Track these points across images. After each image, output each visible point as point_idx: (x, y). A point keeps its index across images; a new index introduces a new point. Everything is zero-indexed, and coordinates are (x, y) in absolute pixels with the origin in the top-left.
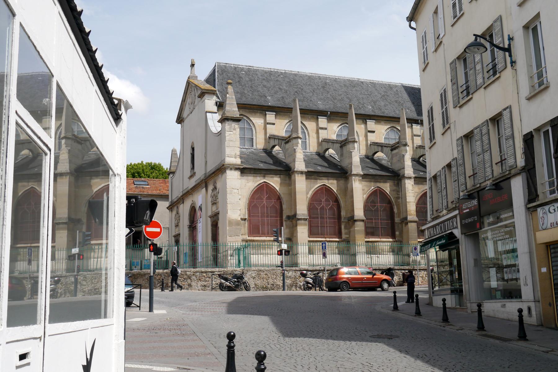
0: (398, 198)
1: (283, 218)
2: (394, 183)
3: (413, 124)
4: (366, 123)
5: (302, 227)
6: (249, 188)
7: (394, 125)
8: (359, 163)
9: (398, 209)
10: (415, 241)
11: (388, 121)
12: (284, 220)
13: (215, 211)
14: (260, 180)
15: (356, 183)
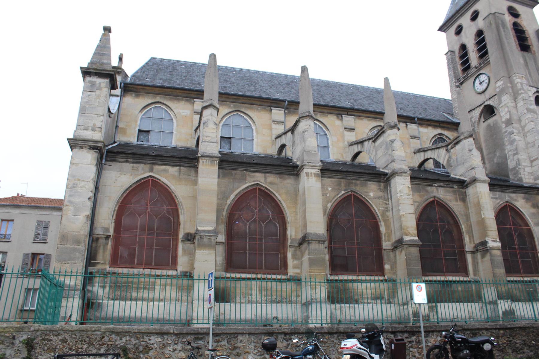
0: (387, 210)
2: (380, 186)
3: (408, 124)
4: (342, 120)
5: (205, 251)
9: (387, 227)
11: (373, 118)
14: (142, 174)
15: (310, 180)
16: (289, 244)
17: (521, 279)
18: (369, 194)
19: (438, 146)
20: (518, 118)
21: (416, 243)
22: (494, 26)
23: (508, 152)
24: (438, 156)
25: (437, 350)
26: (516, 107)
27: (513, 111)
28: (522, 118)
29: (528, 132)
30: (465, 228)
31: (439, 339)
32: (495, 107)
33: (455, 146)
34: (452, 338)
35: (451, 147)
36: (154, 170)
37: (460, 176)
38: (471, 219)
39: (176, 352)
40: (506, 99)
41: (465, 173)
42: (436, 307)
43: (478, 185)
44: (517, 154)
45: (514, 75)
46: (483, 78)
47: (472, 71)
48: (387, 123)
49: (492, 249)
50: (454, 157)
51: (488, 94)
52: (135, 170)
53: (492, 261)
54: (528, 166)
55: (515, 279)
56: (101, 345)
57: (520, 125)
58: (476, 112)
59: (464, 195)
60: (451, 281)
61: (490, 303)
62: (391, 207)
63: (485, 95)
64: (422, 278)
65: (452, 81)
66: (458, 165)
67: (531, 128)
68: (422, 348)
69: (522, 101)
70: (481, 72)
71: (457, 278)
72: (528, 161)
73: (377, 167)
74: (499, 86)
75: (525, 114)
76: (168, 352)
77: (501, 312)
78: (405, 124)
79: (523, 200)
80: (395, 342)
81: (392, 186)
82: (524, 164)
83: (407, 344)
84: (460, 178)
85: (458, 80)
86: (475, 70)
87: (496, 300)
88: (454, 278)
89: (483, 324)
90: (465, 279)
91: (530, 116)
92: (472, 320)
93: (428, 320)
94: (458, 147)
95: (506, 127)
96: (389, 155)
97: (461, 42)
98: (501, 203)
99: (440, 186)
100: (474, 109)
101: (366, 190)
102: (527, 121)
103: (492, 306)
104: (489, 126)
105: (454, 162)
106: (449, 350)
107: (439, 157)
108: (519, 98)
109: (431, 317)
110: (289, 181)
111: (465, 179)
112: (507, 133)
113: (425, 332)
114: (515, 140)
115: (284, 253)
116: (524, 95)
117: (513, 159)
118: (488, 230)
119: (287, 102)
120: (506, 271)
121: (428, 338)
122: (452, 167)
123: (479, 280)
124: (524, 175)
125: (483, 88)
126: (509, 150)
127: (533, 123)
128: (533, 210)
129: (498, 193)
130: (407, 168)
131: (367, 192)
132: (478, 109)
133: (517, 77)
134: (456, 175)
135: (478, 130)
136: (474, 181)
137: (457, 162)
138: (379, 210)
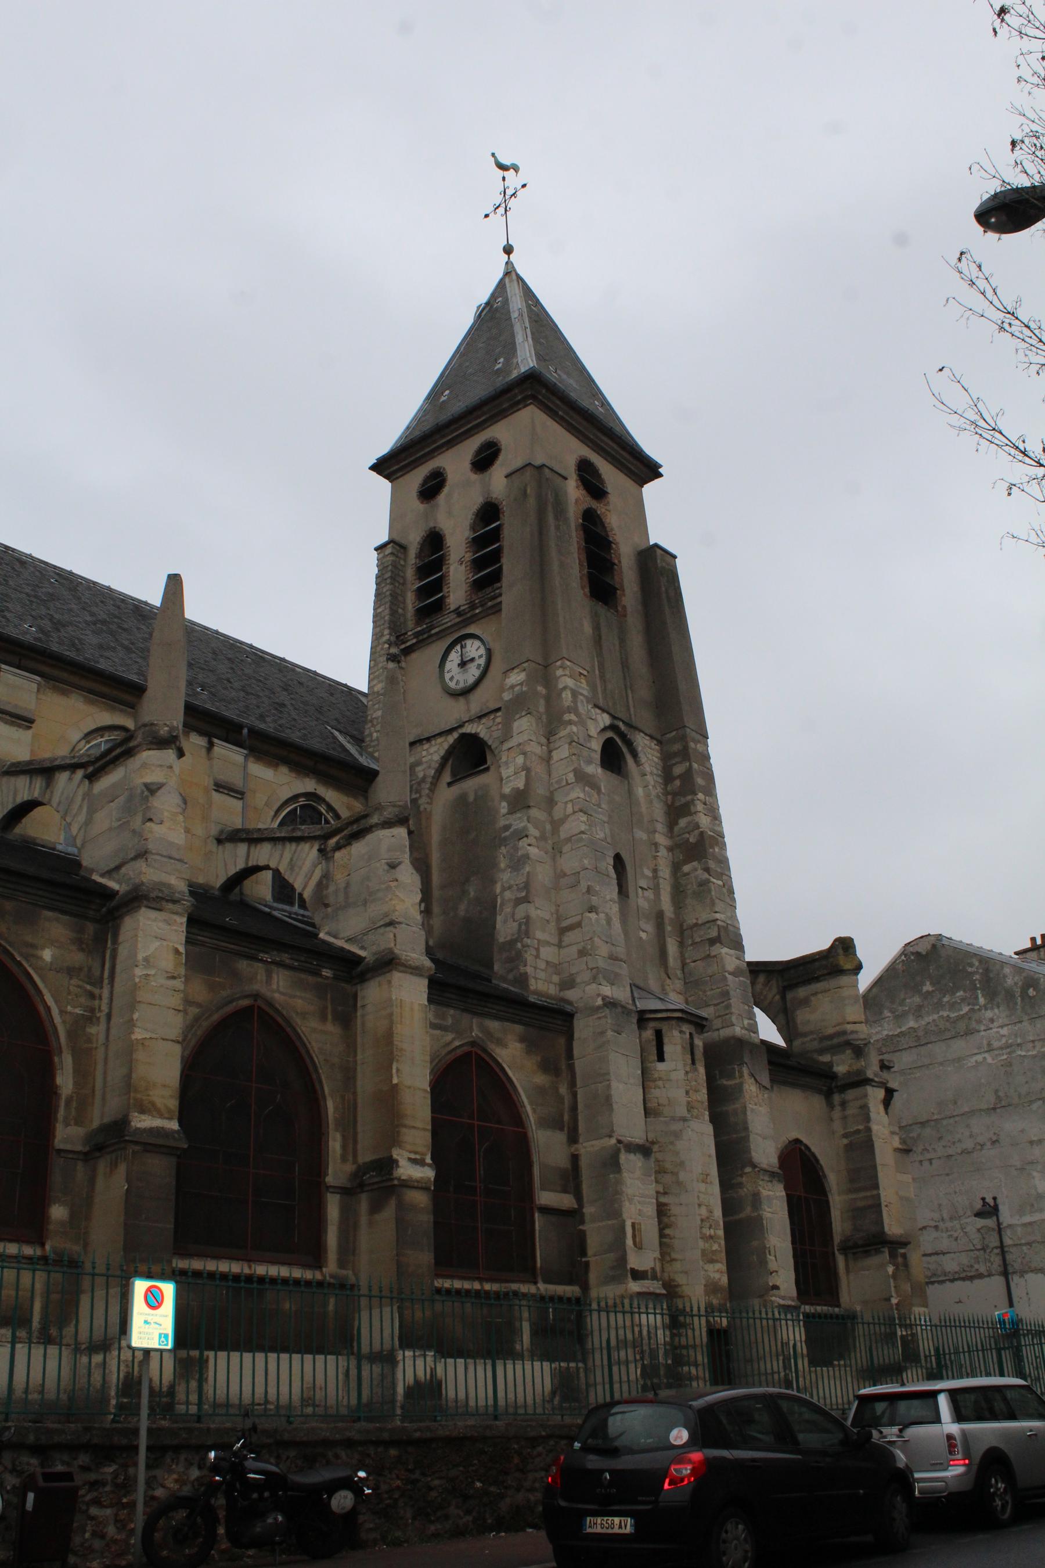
0: (91, 1017)
3: (216, 741)
9: (83, 1074)
17: (477, 1286)
18: (39, 953)
19: (299, 834)
20: (548, 794)
21: (172, 1143)
22: (532, 501)
23: (504, 889)
24: (292, 866)
25: (182, 1514)
26: (547, 759)
27: (539, 769)
28: (559, 797)
29: (569, 840)
30: (336, 1108)
31: (195, 1473)
32: (489, 747)
33: (350, 844)
34: (236, 1469)
35: (337, 843)
37: (349, 940)
38: (359, 1083)
40: (525, 727)
41: (364, 934)
42: (203, 1363)
43: (397, 976)
44: (526, 900)
45: (559, 663)
46: (474, 649)
47: (448, 620)
48: (145, 725)
49: (408, 1184)
50: (339, 877)
51: (478, 701)
53: (401, 1223)
54: (548, 944)
55: (457, 1284)
57: (550, 814)
58: (432, 750)
60: (261, 1280)
61: (375, 1357)
62: (105, 1008)
63: (468, 703)
64: (170, 1262)
65: (382, 635)
67: (577, 831)
68: (132, 1505)
69: (567, 746)
70: (471, 630)
71: (284, 1272)
72: (552, 926)
73: (85, 863)
74: (512, 687)
75: (568, 784)
77: (400, 1390)
78: (206, 739)
79: (518, 1045)
80: (41, 1483)
81: (121, 938)
82: (539, 935)
83: (81, 1492)
84: (347, 946)
85: (399, 637)
86: (455, 619)
87: (393, 1350)
88: (273, 1271)
89: (340, 1424)
90: (308, 1275)
91: (582, 795)
92: (309, 1410)
93: (169, 1407)
94: (358, 848)
95: (511, 812)
96: (134, 831)
97: (432, 525)
98: (457, 1043)
99: (280, 964)
100: (428, 739)
101: (29, 938)
102: (570, 809)
103: (377, 1369)
104: (462, 798)
105: (337, 891)
106: (222, 1514)
108: (562, 733)
109: (181, 1395)
111: (362, 953)
112: (507, 833)
113: (149, 1448)
114: (527, 856)
116: (575, 729)
117: (513, 914)
118: (405, 1126)
120: (435, 1259)
121: (158, 1472)
122: (329, 909)
123: (352, 1280)
124: (535, 968)
125: (465, 681)
127: (584, 818)
128: (541, 1079)
129: (452, 1012)
130: (182, 887)
131: (33, 946)
132: (439, 740)
133: (568, 673)
134: (335, 937)
135: (428, 807)
136: (388, 963)
138: (62, 1012)
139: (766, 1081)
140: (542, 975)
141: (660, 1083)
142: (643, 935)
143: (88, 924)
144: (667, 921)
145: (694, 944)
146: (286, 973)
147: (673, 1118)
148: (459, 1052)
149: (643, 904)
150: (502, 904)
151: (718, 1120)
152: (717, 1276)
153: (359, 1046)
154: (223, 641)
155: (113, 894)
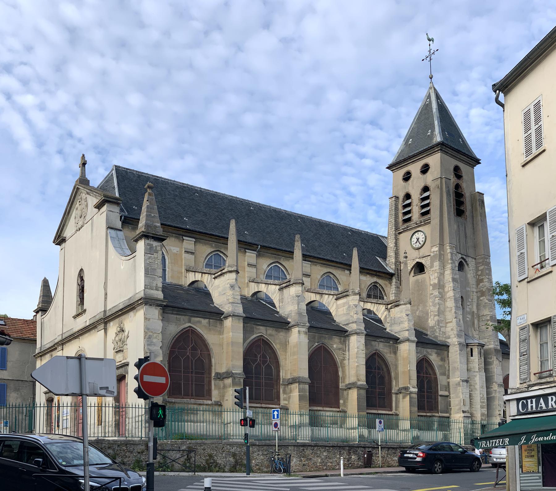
1: (211, 375)
2: (341, 339)
6: (170, 334)
7: (331, 270)
8: (305, 312)
10: (363, 412)
12: (213, 378)
13: (123, 362)
14: (184, 324)
15: (301, 336)
16: (281, 383)
19: (379, 302)
29: (449, 298)
35: (391, 307)
36: (192, 321)
38: (399, 369)
39: (259, 456)
52: (178, 320)
56: (223, 452)
59: (397, 349)
65: (392, 229)
66: (394, 324)
76: (255, 456)
81: (350, 342)
94: (397, 309)
98: (421, 356)
101: (331, 343)
104: (417, 281)
107: (377, 311)
110: (282, 335)
112: (432, 296)
115: (277, 389)
119: (259, 246)
126: (432, 310)
128: (441, 363)
129: (419, 348)
131: (332, 345)
137: (394, 321)
138: (339, 359)
139: (501, 359)
140: (441, 336)
141: (471, 363)
142: (468, 319)
143: (342, 338)
144: (475, 314)
145: (482, 321)
146: (383, 343)
147: (474, 372)
148: (421, 358)
149: (468, 310)
150: (430, 316)
151: (486, 370)
152: (484, 412)
153: (399, 360)
154: (342, 228)
155: (347, 331)
